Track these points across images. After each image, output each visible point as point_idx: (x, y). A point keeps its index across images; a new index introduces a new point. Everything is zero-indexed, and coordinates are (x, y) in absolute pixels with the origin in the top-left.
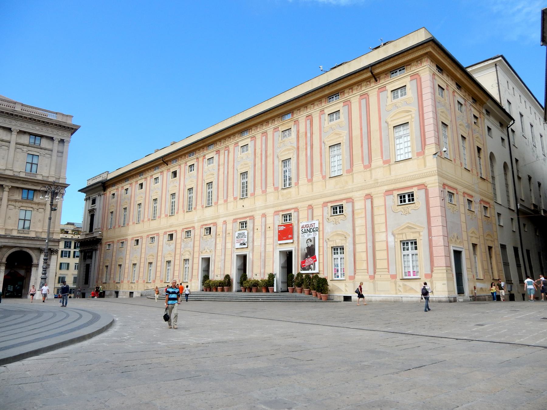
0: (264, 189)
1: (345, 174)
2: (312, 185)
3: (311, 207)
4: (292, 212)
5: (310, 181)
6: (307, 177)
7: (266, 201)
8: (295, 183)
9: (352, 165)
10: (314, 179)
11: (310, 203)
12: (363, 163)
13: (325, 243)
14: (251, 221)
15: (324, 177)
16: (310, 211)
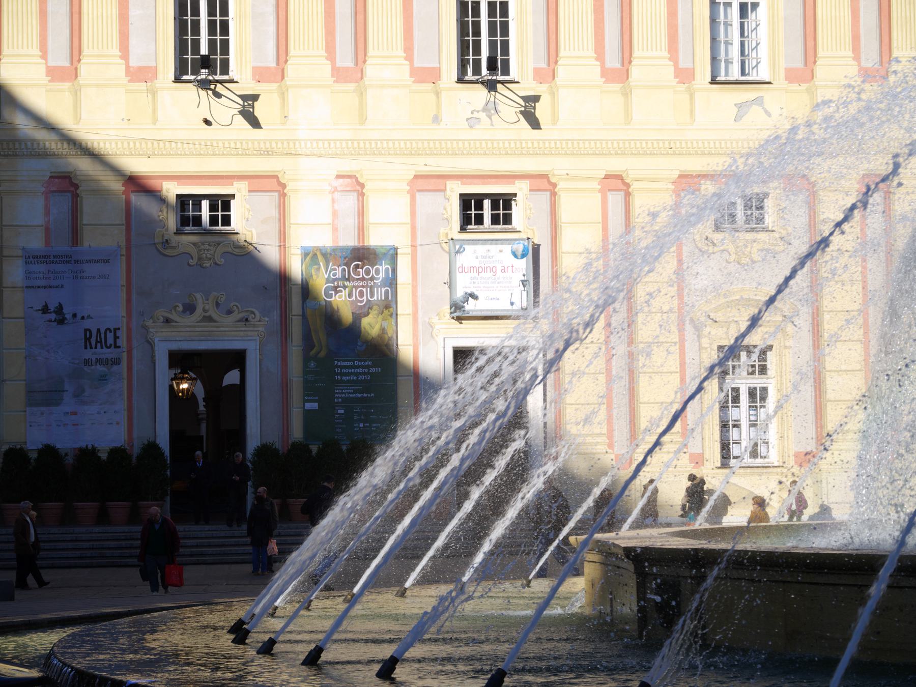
0: (345, 60)
1: (780, 81)
2: (627, 94)
3: (616, 182)
4: (520, 188)
5: (619, 75)
6: (600, 55)
7: (363, 119)
8: (537, 71)
9: (810, 53)
10: (636, 72)
11: (615, 165)
12: (857, 58)
13: (688, 327)
14: (267, 202)
15: (684, 76)
16: (616, 200)
